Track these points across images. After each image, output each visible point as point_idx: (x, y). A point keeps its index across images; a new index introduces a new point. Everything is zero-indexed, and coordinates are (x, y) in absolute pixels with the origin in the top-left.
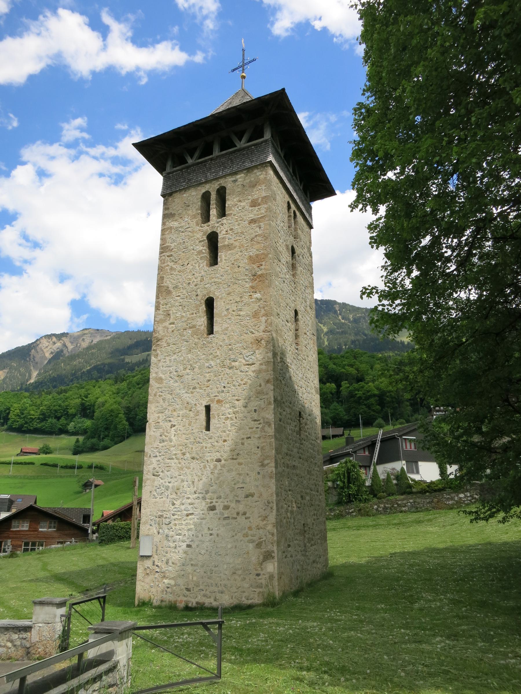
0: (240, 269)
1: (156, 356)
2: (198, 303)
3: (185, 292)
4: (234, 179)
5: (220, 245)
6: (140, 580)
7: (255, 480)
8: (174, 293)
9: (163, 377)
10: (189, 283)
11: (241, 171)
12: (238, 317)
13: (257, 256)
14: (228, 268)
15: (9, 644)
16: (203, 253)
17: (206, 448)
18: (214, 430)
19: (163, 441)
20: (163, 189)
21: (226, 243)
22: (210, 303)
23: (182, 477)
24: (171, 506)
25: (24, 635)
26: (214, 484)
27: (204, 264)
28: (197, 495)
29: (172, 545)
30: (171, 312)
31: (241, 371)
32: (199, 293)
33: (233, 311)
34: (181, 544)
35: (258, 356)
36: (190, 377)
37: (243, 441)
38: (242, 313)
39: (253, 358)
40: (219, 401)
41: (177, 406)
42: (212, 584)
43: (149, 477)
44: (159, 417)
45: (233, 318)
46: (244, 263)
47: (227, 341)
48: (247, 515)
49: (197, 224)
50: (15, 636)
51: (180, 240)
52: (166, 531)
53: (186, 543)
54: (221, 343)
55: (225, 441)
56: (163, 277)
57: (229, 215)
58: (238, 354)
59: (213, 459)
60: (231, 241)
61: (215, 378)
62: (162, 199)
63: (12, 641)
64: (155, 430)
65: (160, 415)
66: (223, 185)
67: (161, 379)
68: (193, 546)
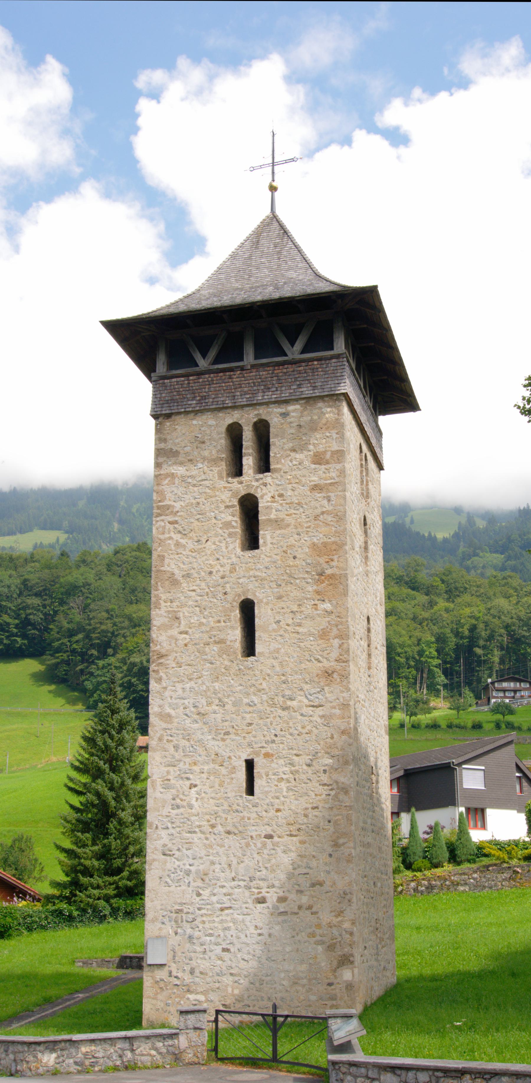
0: (297, 562)
1: (159, 680)
2: (228, 605)
3: (203, 585)
4: (283, 410)
5: (261, 517)
6: (149, 997)
7: (326, 864)
8: (184, 585)
9: (173, 713)
10: (211, 573)
11: (297, 400)
12: (294, 635)
13: (325, 544)
14: (278, 557)
15: (153, 1052)
16: (233, 527)
17: (249, 819)
18: (260, 796)
19: (178, 807)
20: (154, 403)
21: (272, 516)
22: (248, 609)
23: (211, 858)
24: (195, 896)
25: (170, 1042)
26: (262, 869)
27: (236, 543)
28: (236, 883)
29: (199, 949)
30: (181, 615)
31: (302, 715)
32: (228, 590)
33: (288, 625)
34: (213, 947)
35: (328, 695)
36: (219, 716)
37: (307, 812)
38: (301, 630)
39: (320, 697)
40: (267, 755)
41: (199, 758)
42: (262, 997)
43: (155, 857)
44: (168, 773)
45: (287, 635)
46: (303, 552)
47: (278, 669)
48: (314, 910)
49: (221, 477)
50: (160, 1045)
51: (189, 498)
52: (189, 931)
53: (221, 947)
54: (269, 671)
55: (278, 810)
56: (164, 556)
57: (277, 470)
58: (295, 690)
59: (260, 835)
60: (282, 515)
61: (261, 722)
62: (153, 422)
63: (156, 1049)
64: (162, 790)
65: (171, 769)
66: (264, 417)
67: (169, 715)
68: (232, 950)
